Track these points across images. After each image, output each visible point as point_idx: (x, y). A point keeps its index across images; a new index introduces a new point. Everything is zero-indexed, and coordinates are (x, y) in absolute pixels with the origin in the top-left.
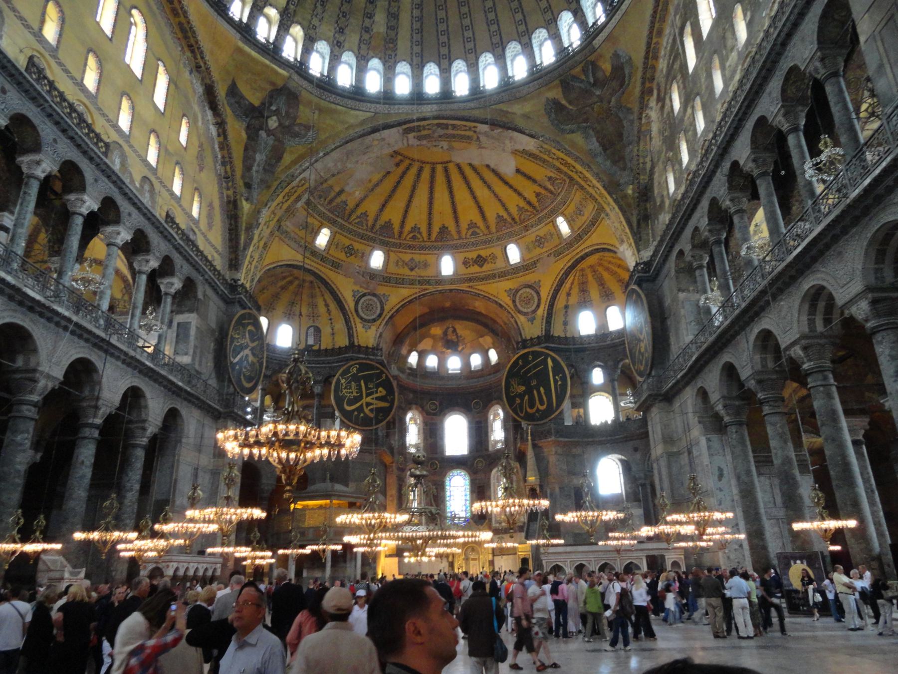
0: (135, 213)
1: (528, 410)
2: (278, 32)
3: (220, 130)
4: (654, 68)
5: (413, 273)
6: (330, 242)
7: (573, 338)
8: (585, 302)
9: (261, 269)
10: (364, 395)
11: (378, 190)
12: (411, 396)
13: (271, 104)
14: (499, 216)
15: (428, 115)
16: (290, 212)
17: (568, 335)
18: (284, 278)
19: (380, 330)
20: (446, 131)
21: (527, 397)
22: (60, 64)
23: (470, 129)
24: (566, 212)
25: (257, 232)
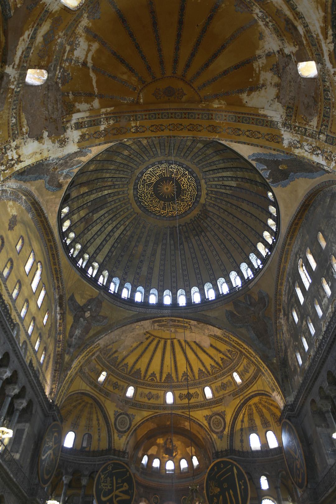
0: (16, 360)
2: (97, 273)
4: (280, 299)
9: (67, 395)
10: (115, 488)
11: (135, 352)
12: (142, 490)
14: (200, 370)
16: (88, 361)
18: (77, 400)
19: (128, 439)
20: (174, 323)
22: (6, 287)
23: (187, 323)
24: (239, 370)
25: (69, 373)
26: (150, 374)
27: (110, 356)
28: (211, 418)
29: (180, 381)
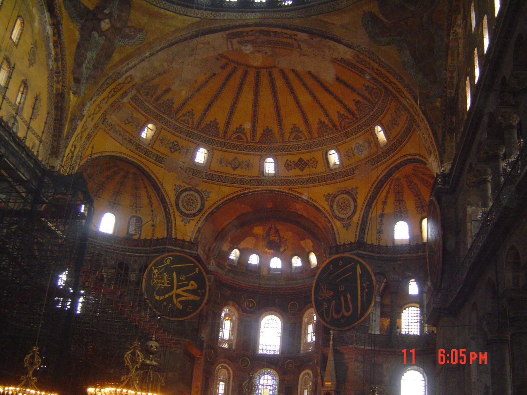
1: (335, 316)
3: (55, 30)
5: (236, 172)
6: (156, 137)
7: (386, 246)
8: (401, 212)
10: (175, 287)
13: (105, 8)
14: (320, 122)
15: (250, 22)
17: (382, 243)
19: (199, 225)
21: (334, 302)
23: (291, 36)
24: (383, 122)
25: (80, 124)
26: (235, 130)
27: (158, 99)
28: (335, 198)
29: (287, 140)
